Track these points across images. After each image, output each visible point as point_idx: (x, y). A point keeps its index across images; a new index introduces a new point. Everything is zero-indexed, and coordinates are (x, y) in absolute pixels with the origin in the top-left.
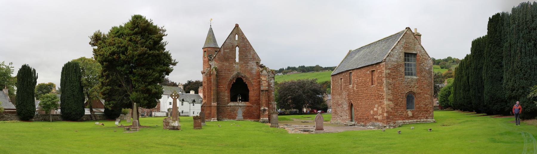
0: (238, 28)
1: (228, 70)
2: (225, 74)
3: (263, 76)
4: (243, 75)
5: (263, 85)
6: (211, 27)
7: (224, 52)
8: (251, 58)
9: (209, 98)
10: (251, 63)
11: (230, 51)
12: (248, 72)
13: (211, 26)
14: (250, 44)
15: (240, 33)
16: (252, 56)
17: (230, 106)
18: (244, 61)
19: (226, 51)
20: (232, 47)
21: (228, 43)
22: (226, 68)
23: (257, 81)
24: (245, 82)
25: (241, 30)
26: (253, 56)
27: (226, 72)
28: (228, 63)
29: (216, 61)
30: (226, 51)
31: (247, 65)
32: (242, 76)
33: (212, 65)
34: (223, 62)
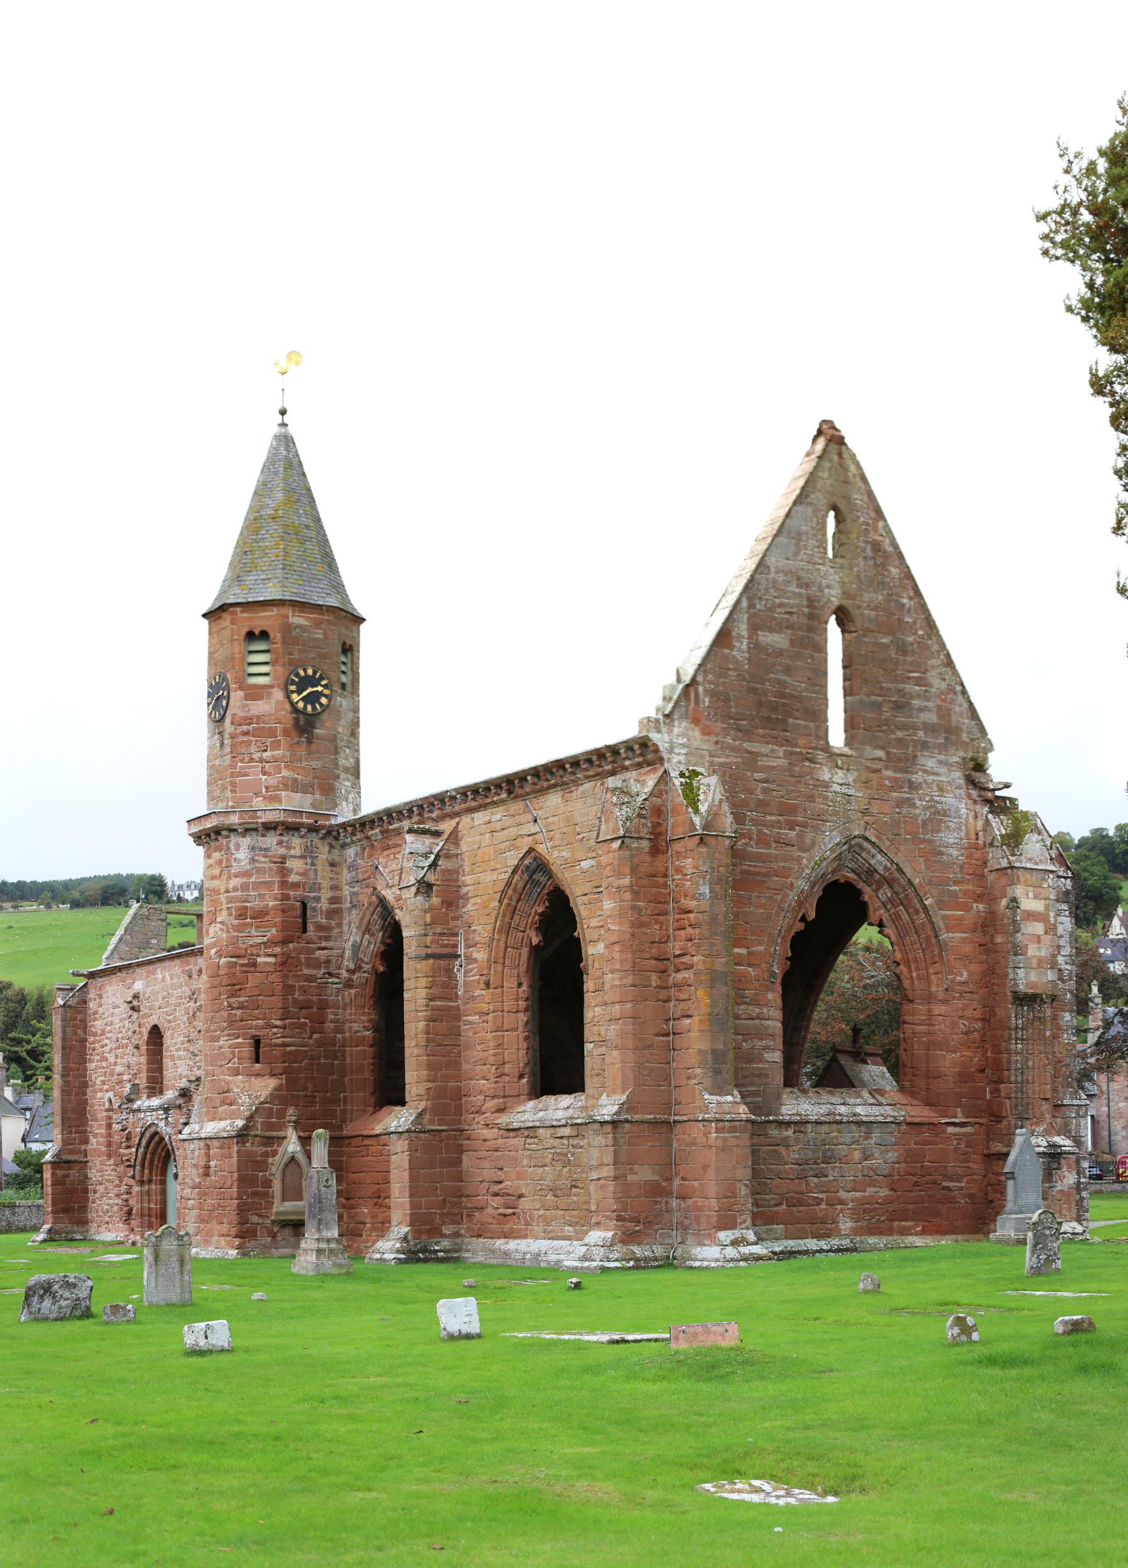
0: (840, 454)
1: (788, 810)
2: (763, 841)
3: (1027, 875)
4: (879, 862)
5: (1030, 953)
8: (930, 729)
9: (650, 1046)
10: (930, 764)
11: (792, 643)
12: (916, 840)
13: (283, 412)
14: (923, 607)
15: (859, 499)
16: (939, 708)
18: (889, 743)
20: (811, 616)
21: (781, 578)
22: (765, 791)
23: (970, 918)
25: (864, 479)
26: (944, 713)
27: (771, 825)
28: (780, 752)
29: (696, 721)
32: (871, 871)
33: (671, 751)
34: (748, 735)
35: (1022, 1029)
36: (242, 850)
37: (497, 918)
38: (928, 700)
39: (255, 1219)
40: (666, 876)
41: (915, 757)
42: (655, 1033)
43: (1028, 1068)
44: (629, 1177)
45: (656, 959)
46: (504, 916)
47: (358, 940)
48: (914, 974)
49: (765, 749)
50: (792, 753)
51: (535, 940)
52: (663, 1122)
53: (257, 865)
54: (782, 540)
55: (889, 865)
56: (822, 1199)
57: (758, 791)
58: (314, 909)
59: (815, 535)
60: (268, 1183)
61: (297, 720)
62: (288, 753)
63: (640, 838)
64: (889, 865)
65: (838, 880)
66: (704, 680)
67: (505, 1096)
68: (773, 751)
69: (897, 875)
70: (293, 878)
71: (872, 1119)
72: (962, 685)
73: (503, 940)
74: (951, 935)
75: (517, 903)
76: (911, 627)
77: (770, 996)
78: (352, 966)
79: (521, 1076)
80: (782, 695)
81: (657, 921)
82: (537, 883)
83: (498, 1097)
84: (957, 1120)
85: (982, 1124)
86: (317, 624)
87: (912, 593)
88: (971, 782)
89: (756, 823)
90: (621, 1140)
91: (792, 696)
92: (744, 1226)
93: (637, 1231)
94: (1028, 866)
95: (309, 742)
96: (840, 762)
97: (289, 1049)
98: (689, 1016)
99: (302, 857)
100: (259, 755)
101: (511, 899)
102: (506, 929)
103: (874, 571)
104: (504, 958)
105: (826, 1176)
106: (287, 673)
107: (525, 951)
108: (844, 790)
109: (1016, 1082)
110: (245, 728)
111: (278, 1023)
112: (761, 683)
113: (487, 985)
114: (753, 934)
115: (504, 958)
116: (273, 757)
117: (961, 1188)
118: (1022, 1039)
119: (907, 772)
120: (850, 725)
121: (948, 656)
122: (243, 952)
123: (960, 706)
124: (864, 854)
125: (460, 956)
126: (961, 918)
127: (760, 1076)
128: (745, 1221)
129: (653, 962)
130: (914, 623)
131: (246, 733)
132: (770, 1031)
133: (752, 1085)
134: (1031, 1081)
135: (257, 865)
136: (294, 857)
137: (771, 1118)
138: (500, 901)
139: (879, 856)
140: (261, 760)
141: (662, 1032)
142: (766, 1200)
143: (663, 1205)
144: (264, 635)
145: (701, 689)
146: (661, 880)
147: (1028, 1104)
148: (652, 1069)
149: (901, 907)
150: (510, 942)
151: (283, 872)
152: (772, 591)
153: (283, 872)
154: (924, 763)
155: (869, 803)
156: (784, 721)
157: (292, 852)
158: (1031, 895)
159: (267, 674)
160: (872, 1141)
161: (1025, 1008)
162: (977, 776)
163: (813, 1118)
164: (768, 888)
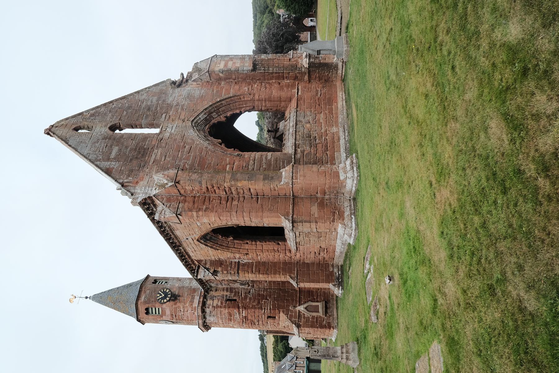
2: (188, 159)
6: (90, 298)
7: (115, 158)
9: (262, 205)
10: (171, 99)
13: (87, 298)
14: (116, 100)
17: (296, 146)
19: (113, 155)
24: (226, 117)
25: (67, 119)
27: (182, 155)
28: (156, 151)
30: (113, 155)
31: (177, 105)
34: (146, 163)
35: (265, 68)
36: (210, 319)
37: (224, 251)
38: (149, 99)
39: (325, 322)
40: (195, 197)
41: (168, 104)
42: (256, 203)
43: (278, 66)
44: (316, 216)
45: (227, 202)
46: (223, 248)
47: (239, 284)
48: (244, 106)
49: (153, 156)
50: (157, 147)
51: (231, 238)
52: (293, 201)
53: (215, 315)
54: (79, 149)
55: (204, 113)
56: (325, 138)
57: (169, 159)
58: (229, 297)
59: (81, 136)
60: (313, 317)
61: (173, 300)
62: (182, 304)
63: (178, 207)
64: (204, 113)
65: (208, 131)
66: (122, 179)
67: (285, 250)
68: (155, 154)
69: (207, 110)
70: (219, 304)
71: (295, 120)
72: (146, 88)
73: (232, 249)
74: (231, 93)
75: (218, 244)
76: (123, 104)
77: (246, 156)
78: (247, 285)
79: (279, 244)
80: (135, 149)
81: (212, 201)
82: (211, 238)
83: (285, 252)
84: (296, 91)
85: (298, 83)
86: (145, 292)
87: (111, 104)
88: (180, 85)
89: (180, 160)
90: (300, 219)
91: (136, 146)
92: (337, 168)
93: (339, 213)
94: (208, 66)
95: (179, 296)
96: (164, 130)
97: (271, 308)
98: (250, 189)
99: (213, 301)
100: (182, 312)
101: (217, 246)
102: (228, 248)
103: (100, 116)
104: (238, 248)
105: (316, 137)
106: (158, 303)
107: (236, 241)
108: (174, 128)
109: (283, 70)
110: (174, 316)
111: (263, 311)
112: (129, 157)
113: (247, 254)
114: (222, 162)
115: (238, 248)
116: (183, 308)
117: (321, 90)
118: (268, 68)
119: (172, 107)
120: (151, 126)
121: (136, 93)
122: (242, 320)
123: (153, 89)
124: (199, 122)
125: (239, 261)
126: (226, 90)
127: (276, 161)
128: (336, 168)
129: (228, 203)
130: (122, 103)
131: (176, 316)
132: (260, 157)
133: (280, 164)
134: (283, 65)
135: (215, 315)
136: (213, 303)
137: (293, 157)
138: (218, 250)
139: (200, 116)
140: (184, 312)
141: (256, 200)
142: (325, 159)
143: (327, 201)
144: (147, 309)
145: (125, 181)
146: (196, 198)
147: (291, 66)
148: (271, 205)
149: (220, 109)
150: (232, 246)
151: (217, 307)
152: (97, 152)
153: (217, 307)
154: (170, 101)
155: (181, 119)
156: (145, 149)
157: (211, 304)
158: (219, 65)
159: (159, 309)
160: (303, 120)
161: (257, 67)
162: (177, 84)
163: (294, 141)
164: (206, 156)
